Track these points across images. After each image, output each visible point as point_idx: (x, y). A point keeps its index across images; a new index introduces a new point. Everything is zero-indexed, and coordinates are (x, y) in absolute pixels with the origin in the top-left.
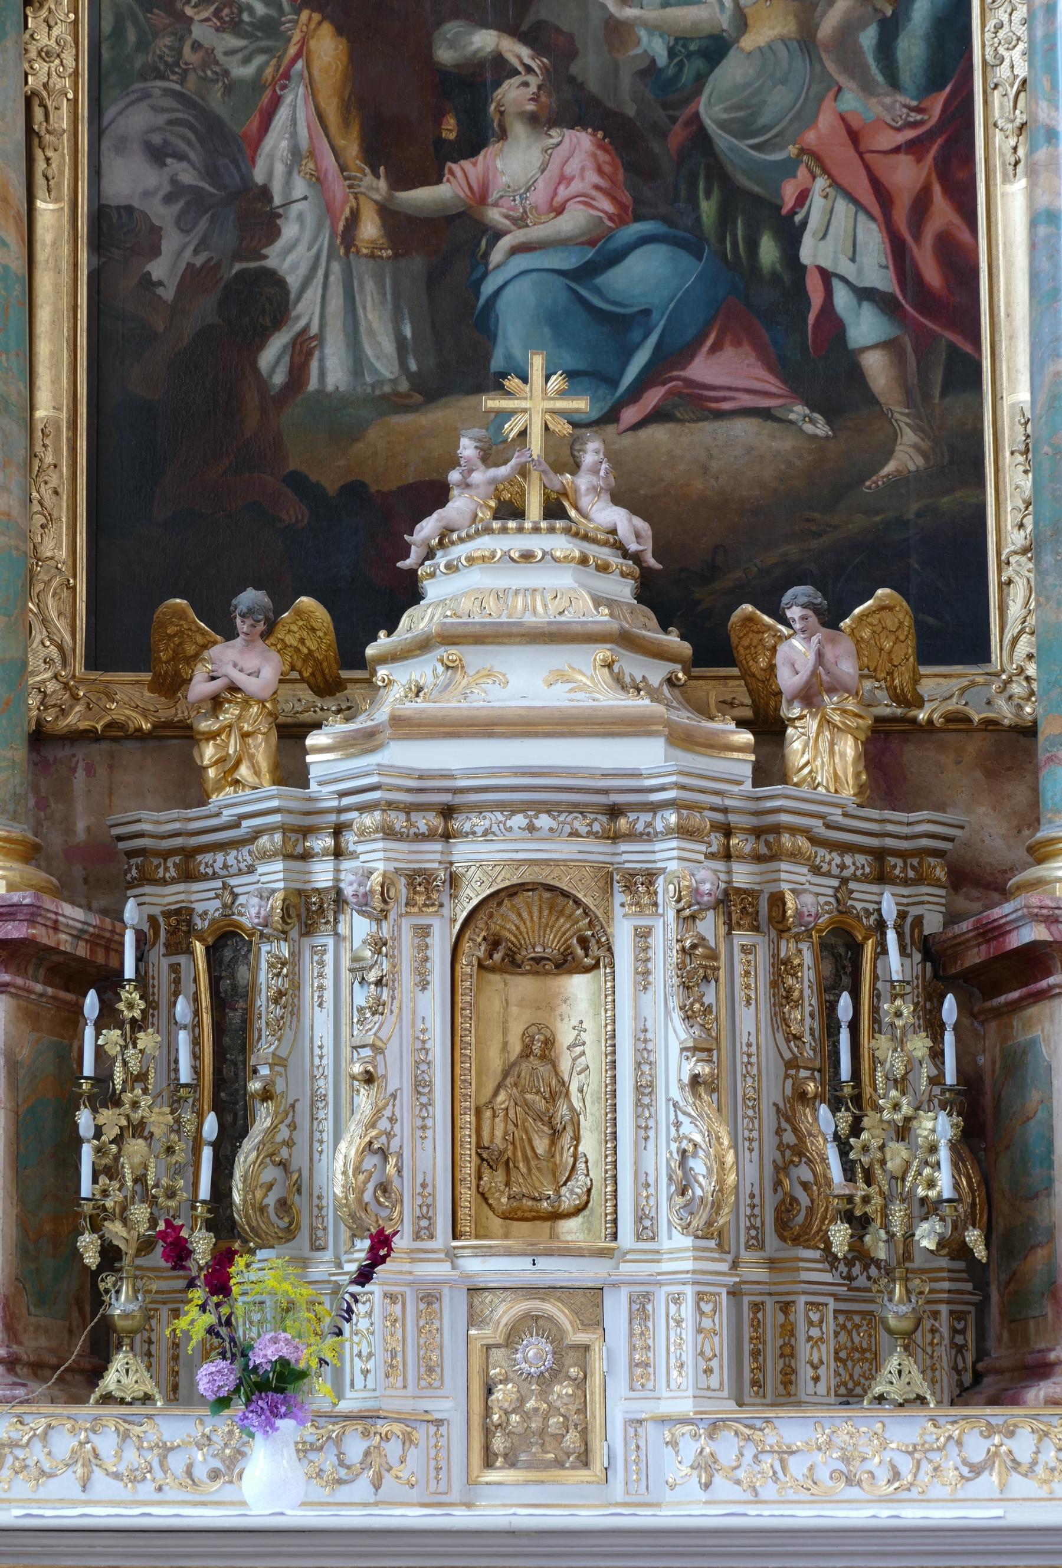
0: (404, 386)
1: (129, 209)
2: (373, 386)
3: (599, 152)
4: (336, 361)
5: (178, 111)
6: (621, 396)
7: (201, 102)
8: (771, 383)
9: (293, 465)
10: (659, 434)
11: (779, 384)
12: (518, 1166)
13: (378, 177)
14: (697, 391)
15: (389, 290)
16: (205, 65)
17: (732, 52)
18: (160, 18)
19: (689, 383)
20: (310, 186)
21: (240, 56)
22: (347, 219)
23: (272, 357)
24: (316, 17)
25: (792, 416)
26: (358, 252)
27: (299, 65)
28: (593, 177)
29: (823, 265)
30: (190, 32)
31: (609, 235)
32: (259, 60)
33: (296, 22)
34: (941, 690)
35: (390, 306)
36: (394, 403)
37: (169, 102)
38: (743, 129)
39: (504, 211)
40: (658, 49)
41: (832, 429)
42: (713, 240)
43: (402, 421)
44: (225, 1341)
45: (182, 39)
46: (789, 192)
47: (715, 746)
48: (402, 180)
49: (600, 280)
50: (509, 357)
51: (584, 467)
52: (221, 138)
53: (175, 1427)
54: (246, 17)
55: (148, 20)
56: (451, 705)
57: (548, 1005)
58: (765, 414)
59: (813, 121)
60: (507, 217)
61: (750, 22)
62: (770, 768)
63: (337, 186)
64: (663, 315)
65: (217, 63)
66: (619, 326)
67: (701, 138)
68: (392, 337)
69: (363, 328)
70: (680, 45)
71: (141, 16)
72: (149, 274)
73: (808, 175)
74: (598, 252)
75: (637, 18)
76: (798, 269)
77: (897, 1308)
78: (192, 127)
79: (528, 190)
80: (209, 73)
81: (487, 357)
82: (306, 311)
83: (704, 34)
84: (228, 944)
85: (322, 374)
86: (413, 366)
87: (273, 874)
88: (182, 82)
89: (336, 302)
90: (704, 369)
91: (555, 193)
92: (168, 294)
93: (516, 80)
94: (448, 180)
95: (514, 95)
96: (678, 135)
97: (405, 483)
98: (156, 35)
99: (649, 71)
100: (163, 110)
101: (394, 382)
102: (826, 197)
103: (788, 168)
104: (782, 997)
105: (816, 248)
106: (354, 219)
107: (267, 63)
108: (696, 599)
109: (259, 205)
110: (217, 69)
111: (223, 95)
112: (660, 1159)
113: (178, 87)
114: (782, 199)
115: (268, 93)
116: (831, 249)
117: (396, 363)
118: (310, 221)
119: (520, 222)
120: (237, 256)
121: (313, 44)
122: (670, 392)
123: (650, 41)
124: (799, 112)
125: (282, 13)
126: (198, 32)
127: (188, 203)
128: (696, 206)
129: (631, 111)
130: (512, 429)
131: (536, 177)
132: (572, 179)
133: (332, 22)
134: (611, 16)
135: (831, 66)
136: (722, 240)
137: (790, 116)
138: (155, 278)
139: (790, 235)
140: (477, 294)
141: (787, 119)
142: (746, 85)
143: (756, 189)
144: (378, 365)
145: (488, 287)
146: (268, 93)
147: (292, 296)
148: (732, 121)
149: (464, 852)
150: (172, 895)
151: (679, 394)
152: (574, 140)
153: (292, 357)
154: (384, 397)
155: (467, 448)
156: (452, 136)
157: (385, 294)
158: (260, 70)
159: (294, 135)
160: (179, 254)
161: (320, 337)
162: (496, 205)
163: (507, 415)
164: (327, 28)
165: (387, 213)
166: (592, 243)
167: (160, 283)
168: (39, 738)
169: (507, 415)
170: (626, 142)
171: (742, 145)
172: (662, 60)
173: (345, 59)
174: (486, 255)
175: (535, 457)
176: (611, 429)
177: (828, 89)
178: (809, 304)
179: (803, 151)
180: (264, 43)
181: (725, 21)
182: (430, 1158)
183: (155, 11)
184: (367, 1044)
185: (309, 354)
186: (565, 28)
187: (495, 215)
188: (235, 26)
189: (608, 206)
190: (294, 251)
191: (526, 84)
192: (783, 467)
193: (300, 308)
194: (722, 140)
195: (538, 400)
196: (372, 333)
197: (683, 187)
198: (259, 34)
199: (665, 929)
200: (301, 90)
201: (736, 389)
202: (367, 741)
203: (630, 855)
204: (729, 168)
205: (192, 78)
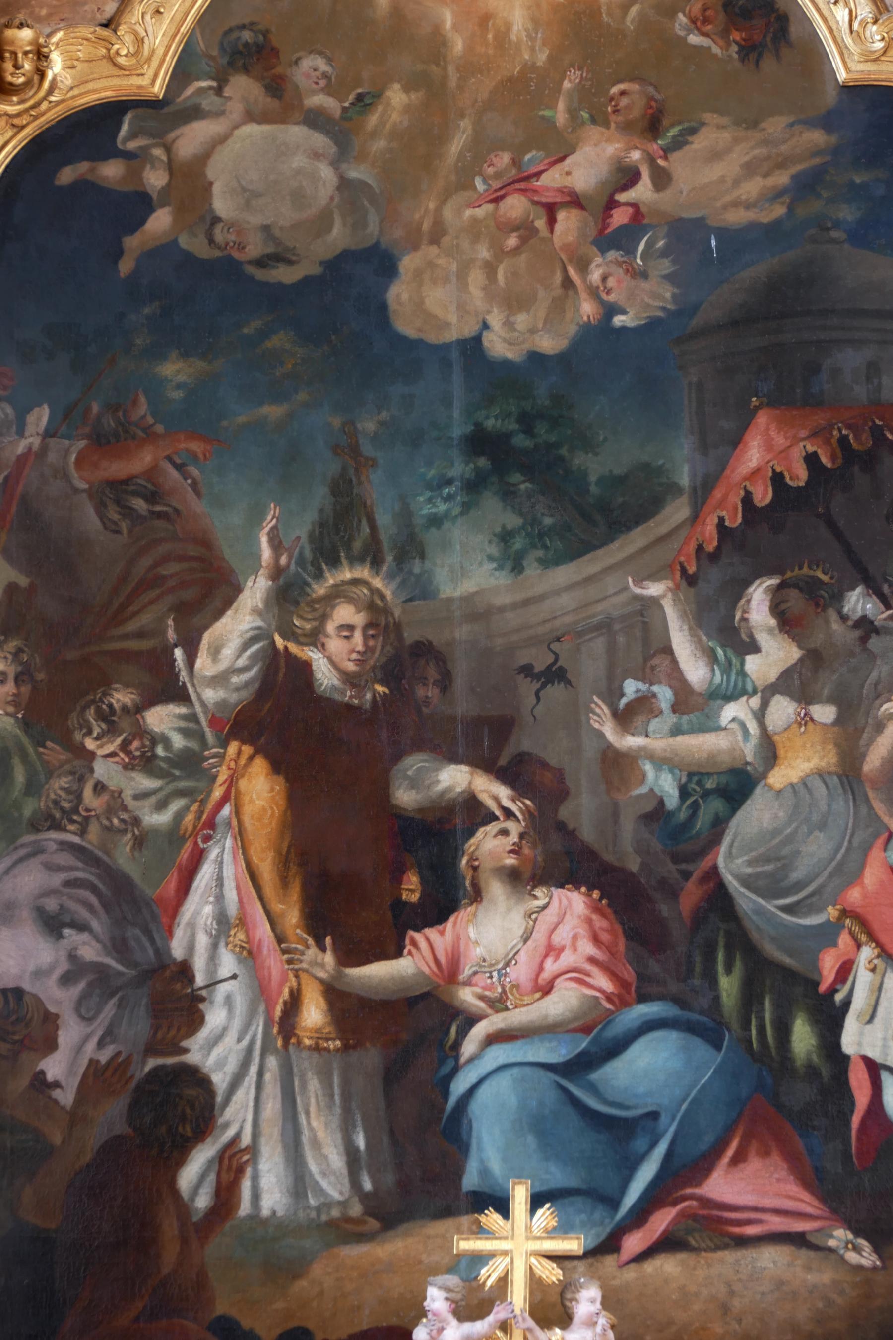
0: (356, 1210)
1: (18, 993)
2: (318, 1209)
3: (594, 917)
4: (273, 1179)
5: (77, 869)
6: (623, 1219)
7: (105, 858)
8: (807, 1202)
9: (221, 1308)
10: (668, 1266)
11: (816, 1203)
13: (324, 950)
14: (716, 1213)
15: (337, 1091)
16: (110, 811)
17: (758, 790)
18: (54, 753)
19: (706, 1202)
20: (240, 961)
21: (153, 799)
22: (285, 1003)
23: (194, 1173)
24: (247, 750)
25: (832, 1243)
26: (299, 1043)
27: (226, 811)
28: (588, 948)
29: (870, 1054)
30: (92, 771)
31: (607, 1018)
32: (176, 805)
33: (222, 757)
35: (338, 1110)
36: (342, 1231)
37: (65, 859)
38: (771, 885)
39: (478, 990)
40: (667, 786)
41: (880, 1258)
42: (735, 1025)
43: (353, 1252)
45: (81, 780)
46: (829, 965)
48: (354, 953)
49: (595, 1076)
50: (485, 1172)
51: (577, 1320)
54: (160, 751)
55: (39, 755)
58: (798, 1240)
59: (857, 877)
60: (482, 998)
61: (781, 753)
63: (274, 962)
64: (673, 1119)
65: (125, 809)
66: (620, 1131)
67: (719, 898)
68: (342, 1149)
69: (305, 1138)
70: (695, 780)
71: (31, 750)
72: (43, 1073)
73: (851, 943)
74: (592, 1042)
75: (641, 749)
76: (837, 1059)
78: (94, 890)
79: (507, 964)
80: (115, 821)
81: (458, 1173)
82: (236, 1117)
83: (724, 767)
85: (256, 1196)
86: (368, 1185)
88: (83, 833)
89: (272, 1106)
90: (723, 1186)
91: (541, 968)
92: (66, 1097)
93: (492, 828)
94: (410, 953)
95: (491, 846)
96: (691, 895)
97: (357, 1329)
98: (50, 774)
99: (656, 814)
100: (59, 869)
101: (344, 1204)
102: (873, 970)
103: (826, 935)
105: (861, 1034)
106: (294, 1004)
107: (187, 808)
109: (178, 986)
110: (125, 816)
111: (133, 848)
113: (76, 839)
114: (820, 973)
115: (188, 845)
116: (880, 1035)
117: (346, 1181)
118: (240, 1004)
119: (498, 1004)
120: (151, 1050)
121: (243, 784)
122: (682, 1215)
123: (657, 778)
124: (841, 864)
125: (204, 745)
126: (102, 770)
127: (90, 985)
128: (714, 982)
129: (634, 865)
130: (489, 1275)
131: (519, 948)
132: (562, 949)
133: (267, 757)
134: (610, 746)
135: (879, 807)
136: (746, 1026)
137: (829, 869)
138: (50, 1077)
139: (830, 1017)
140: (446, 1093)
141: (826, 873)
142: (775, 832)
143: (787, 961)
144: (324, 1184)
145: (459, 1086)
146: (188, 845)
147: (219, 1099)
148: (757, 876)
151: (694, 1217)
152: (565, 901)
153: (219, 1175)
154: (332, 1224)
155: (436, 1300)
156: (415, 898)
157: (332, 1096)
158: (179, 817)
159: (220, 898)
160: (79, 1049)
161: (253, 1150)
162: (468, 983)
163: (480, 1259)
164: (260, 765)
165: (334, 994)
166: (586, 1030)
167: (56, 1085)
169: (480, 1259)
171: (770, 906)
172: (672, 799)
173: (282, 802)
174: (457, 1046)
175: (518, 1311)
176: (610, 1261)
177: (876, 836)
178: (853, 1103)
179: (844, 913)
180: (183, 784)
181: (749, 751)
183: (49, 744)
185: (240, 1171)
186: (553, 762)
187: (467, 996)
188: (146, 763)
189: (604, 983)
190: (222, 1042)
191: (504, 832)
192: (820, 1305)
193: (229, 1113)
194: (746, 901)
196: (316, 1144)
197: (698, 959)
198: (177, 773)
200: (229, 843)
201: (763, 1210)
204: (755, 935)
205: (94, 829)
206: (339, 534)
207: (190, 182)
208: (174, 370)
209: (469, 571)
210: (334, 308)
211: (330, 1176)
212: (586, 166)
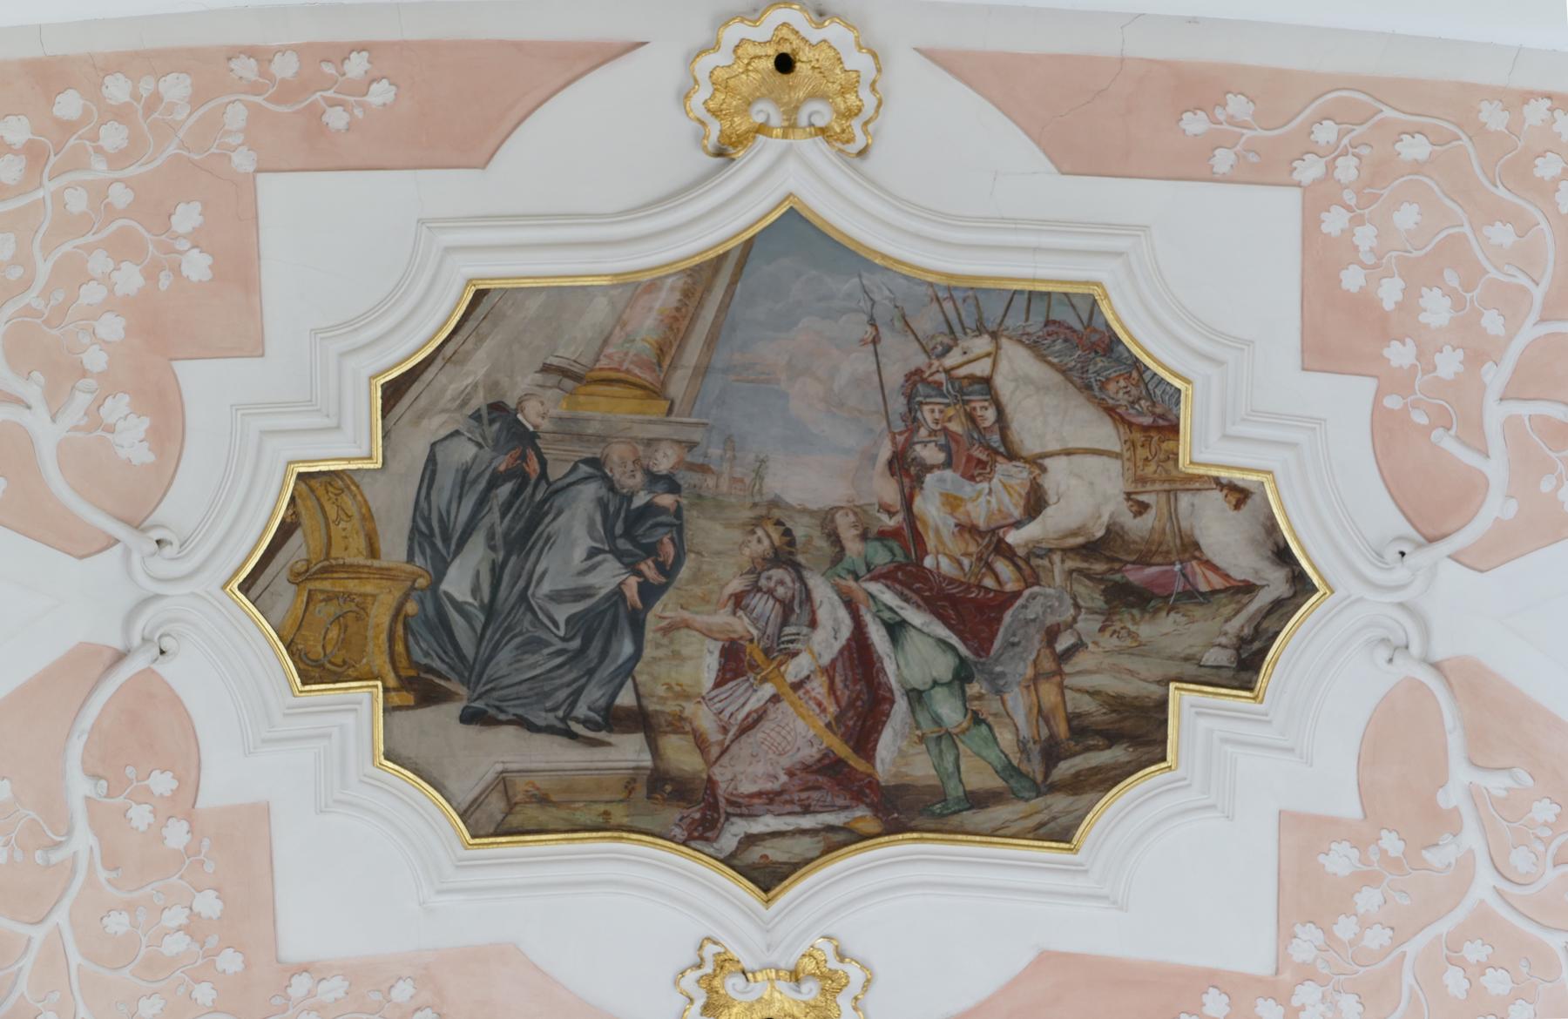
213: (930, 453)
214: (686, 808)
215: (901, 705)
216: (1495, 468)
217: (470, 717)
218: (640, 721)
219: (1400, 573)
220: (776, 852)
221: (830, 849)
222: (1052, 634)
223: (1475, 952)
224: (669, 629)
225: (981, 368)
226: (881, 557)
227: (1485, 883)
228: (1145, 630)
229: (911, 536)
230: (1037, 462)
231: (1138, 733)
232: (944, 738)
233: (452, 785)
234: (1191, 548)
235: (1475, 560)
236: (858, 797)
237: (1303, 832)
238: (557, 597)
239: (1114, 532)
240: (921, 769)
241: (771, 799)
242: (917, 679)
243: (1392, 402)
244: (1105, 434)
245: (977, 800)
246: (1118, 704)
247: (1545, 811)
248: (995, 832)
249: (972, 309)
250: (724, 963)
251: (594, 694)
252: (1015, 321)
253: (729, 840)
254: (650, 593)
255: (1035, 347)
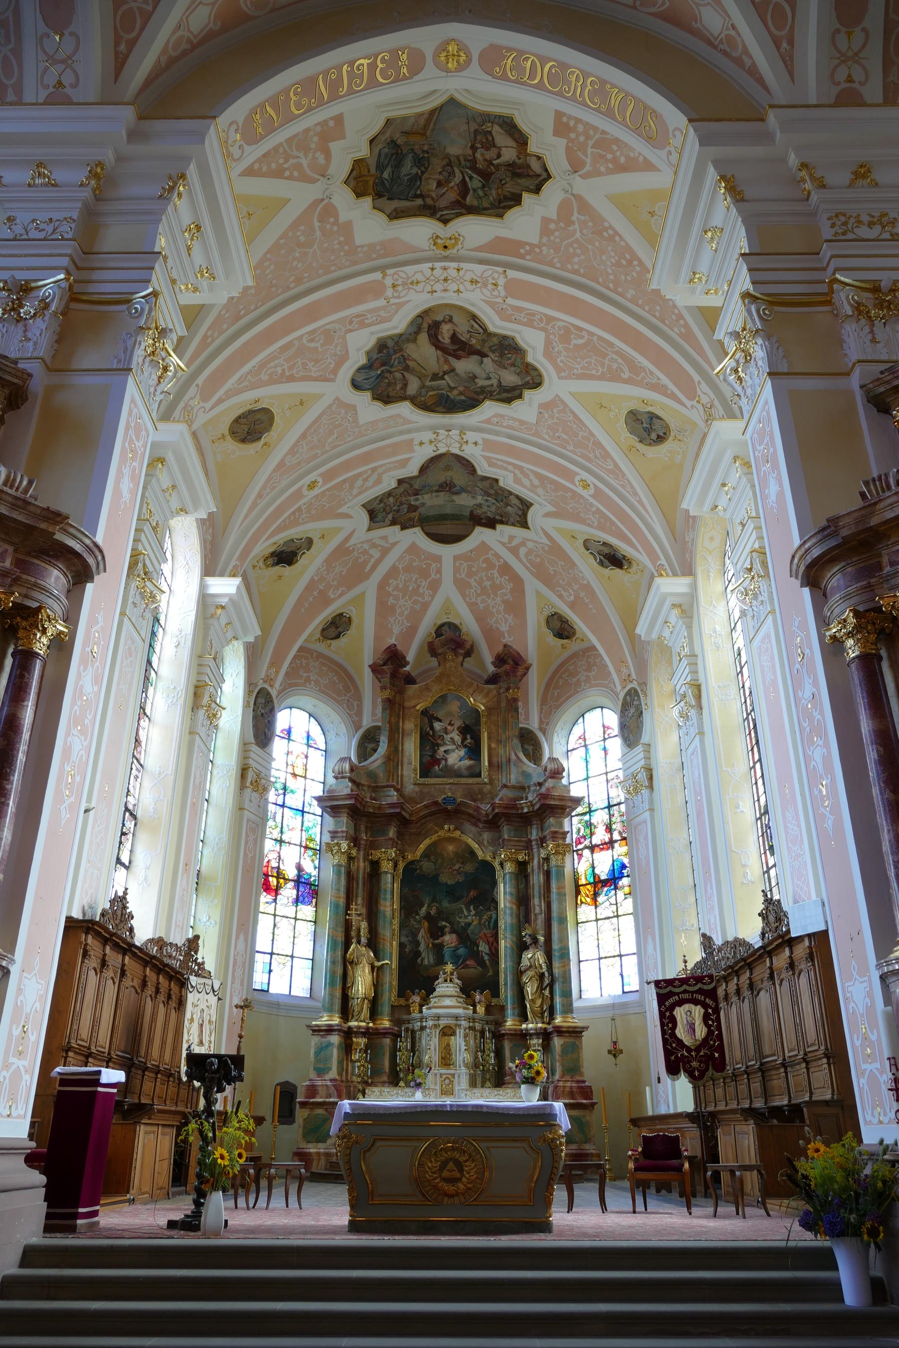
12: (446, 1060)
34: (494, 1001)
44: (413, 1080)
47: (468, 1009)
52: (414, 935)
53: (408, 1090)
56: (439, 1005)
57: (449, 1040)
62: (475, 1011)
66: (458, 957)
70: (466, 924)
77: (488, 1077)
82: (423, 955)
84: (413, 1032)
87: (419, 1024)
90: (468, 962)
95: (447, 930)
104: (475, 1039)
108: (467, 991)
112: (462, 1058)
131: (449, 939)
149: (440, 1022)
150: (407, 1026)
168: (392, 1006)
170: (459, 935)
182: (436, 1058)
184: (430, 1046)
190: (422, 948)
195: (449, 967)
199: (462, 1031)
202: (429, 1008)
203: (459, 1022)
206: (434, 900)
207: (421, 867)
208: (419, 885)
209: (445, 904)
210: (433, 880)
211: (432, 961)
212: (457, 867)
213: (479, 145)
214: (430, 211)
215: (471, 192)
216: (588, 161)
217: (388, 199)
218: (422, 196)
219: (568, 178)
220: (447, 217)
221: (457, 216)
222: (501, 180)
223: (575, 245)
224: (428, 178)
225: (489, 129)
226: (468, 164)
227: (578, 235)
228: (519, 181)
229: (474, 161)
230: (500, 148)
231: (517, 200)
232: (479, 198)
233: (386, 212)
234: (529, 167)
235: (583, 177)
236: (463, 207)
237: (546, 221)
238: (405, 175)
239: (514, 162)
240: (475, 203)
241: (446, 208)
242: (475, 187)
243: (570, 144)
244: (513, 144)
245: (485, 209)
246: (513, 194)
247: (590, 224)
248: (489, 215)
249: (488, 118)
250: (437, 237)
251: (412, 192)
252: (497, 120)
253: (438, 216)
254: (423, 173)
255: (500, 126)
